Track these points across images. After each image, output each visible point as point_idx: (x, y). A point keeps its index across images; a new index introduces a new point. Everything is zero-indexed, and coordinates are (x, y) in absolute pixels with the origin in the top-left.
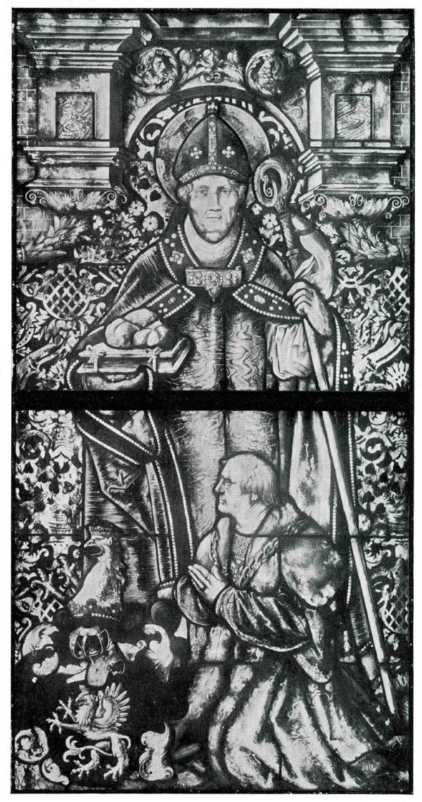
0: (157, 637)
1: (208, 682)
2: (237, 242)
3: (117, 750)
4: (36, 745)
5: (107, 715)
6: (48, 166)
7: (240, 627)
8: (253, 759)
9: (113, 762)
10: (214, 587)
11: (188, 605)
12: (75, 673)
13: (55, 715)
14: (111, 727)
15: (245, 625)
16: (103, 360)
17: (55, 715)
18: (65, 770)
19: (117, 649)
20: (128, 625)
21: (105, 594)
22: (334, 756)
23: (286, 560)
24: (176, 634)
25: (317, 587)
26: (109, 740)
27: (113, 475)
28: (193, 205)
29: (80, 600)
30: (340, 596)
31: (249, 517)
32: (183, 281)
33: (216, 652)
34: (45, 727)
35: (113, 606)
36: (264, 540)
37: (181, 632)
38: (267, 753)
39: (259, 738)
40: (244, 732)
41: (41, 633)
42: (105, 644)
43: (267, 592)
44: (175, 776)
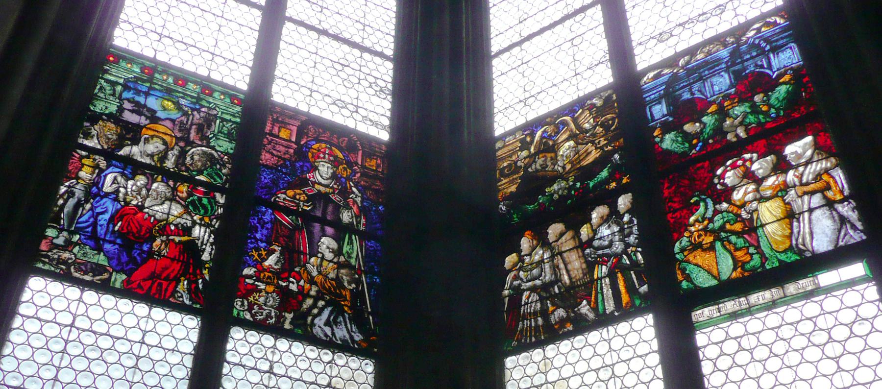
0: (293, 283)
1: (309, 302)
3: (273, 314)
4: (243, 305)
9: (272, 318)
10: (315, 273)
11: (305, 276)
12: (262, 286)
14: (272, 307)
15: (324, 288)
16: (284, 199)
18: (252, 316)
21: (276, 264)
22: (351, 337)
25: (350, 283)
29: (267, 263)
30: (357, 288)
31: (329, 256)
32: (313, 187)
33: (313, 293)
34: (248, 300)
37: (302, 283)
38: (328, 330)
39: (325, 325)
40: (320, 321)
43: (332, 279)
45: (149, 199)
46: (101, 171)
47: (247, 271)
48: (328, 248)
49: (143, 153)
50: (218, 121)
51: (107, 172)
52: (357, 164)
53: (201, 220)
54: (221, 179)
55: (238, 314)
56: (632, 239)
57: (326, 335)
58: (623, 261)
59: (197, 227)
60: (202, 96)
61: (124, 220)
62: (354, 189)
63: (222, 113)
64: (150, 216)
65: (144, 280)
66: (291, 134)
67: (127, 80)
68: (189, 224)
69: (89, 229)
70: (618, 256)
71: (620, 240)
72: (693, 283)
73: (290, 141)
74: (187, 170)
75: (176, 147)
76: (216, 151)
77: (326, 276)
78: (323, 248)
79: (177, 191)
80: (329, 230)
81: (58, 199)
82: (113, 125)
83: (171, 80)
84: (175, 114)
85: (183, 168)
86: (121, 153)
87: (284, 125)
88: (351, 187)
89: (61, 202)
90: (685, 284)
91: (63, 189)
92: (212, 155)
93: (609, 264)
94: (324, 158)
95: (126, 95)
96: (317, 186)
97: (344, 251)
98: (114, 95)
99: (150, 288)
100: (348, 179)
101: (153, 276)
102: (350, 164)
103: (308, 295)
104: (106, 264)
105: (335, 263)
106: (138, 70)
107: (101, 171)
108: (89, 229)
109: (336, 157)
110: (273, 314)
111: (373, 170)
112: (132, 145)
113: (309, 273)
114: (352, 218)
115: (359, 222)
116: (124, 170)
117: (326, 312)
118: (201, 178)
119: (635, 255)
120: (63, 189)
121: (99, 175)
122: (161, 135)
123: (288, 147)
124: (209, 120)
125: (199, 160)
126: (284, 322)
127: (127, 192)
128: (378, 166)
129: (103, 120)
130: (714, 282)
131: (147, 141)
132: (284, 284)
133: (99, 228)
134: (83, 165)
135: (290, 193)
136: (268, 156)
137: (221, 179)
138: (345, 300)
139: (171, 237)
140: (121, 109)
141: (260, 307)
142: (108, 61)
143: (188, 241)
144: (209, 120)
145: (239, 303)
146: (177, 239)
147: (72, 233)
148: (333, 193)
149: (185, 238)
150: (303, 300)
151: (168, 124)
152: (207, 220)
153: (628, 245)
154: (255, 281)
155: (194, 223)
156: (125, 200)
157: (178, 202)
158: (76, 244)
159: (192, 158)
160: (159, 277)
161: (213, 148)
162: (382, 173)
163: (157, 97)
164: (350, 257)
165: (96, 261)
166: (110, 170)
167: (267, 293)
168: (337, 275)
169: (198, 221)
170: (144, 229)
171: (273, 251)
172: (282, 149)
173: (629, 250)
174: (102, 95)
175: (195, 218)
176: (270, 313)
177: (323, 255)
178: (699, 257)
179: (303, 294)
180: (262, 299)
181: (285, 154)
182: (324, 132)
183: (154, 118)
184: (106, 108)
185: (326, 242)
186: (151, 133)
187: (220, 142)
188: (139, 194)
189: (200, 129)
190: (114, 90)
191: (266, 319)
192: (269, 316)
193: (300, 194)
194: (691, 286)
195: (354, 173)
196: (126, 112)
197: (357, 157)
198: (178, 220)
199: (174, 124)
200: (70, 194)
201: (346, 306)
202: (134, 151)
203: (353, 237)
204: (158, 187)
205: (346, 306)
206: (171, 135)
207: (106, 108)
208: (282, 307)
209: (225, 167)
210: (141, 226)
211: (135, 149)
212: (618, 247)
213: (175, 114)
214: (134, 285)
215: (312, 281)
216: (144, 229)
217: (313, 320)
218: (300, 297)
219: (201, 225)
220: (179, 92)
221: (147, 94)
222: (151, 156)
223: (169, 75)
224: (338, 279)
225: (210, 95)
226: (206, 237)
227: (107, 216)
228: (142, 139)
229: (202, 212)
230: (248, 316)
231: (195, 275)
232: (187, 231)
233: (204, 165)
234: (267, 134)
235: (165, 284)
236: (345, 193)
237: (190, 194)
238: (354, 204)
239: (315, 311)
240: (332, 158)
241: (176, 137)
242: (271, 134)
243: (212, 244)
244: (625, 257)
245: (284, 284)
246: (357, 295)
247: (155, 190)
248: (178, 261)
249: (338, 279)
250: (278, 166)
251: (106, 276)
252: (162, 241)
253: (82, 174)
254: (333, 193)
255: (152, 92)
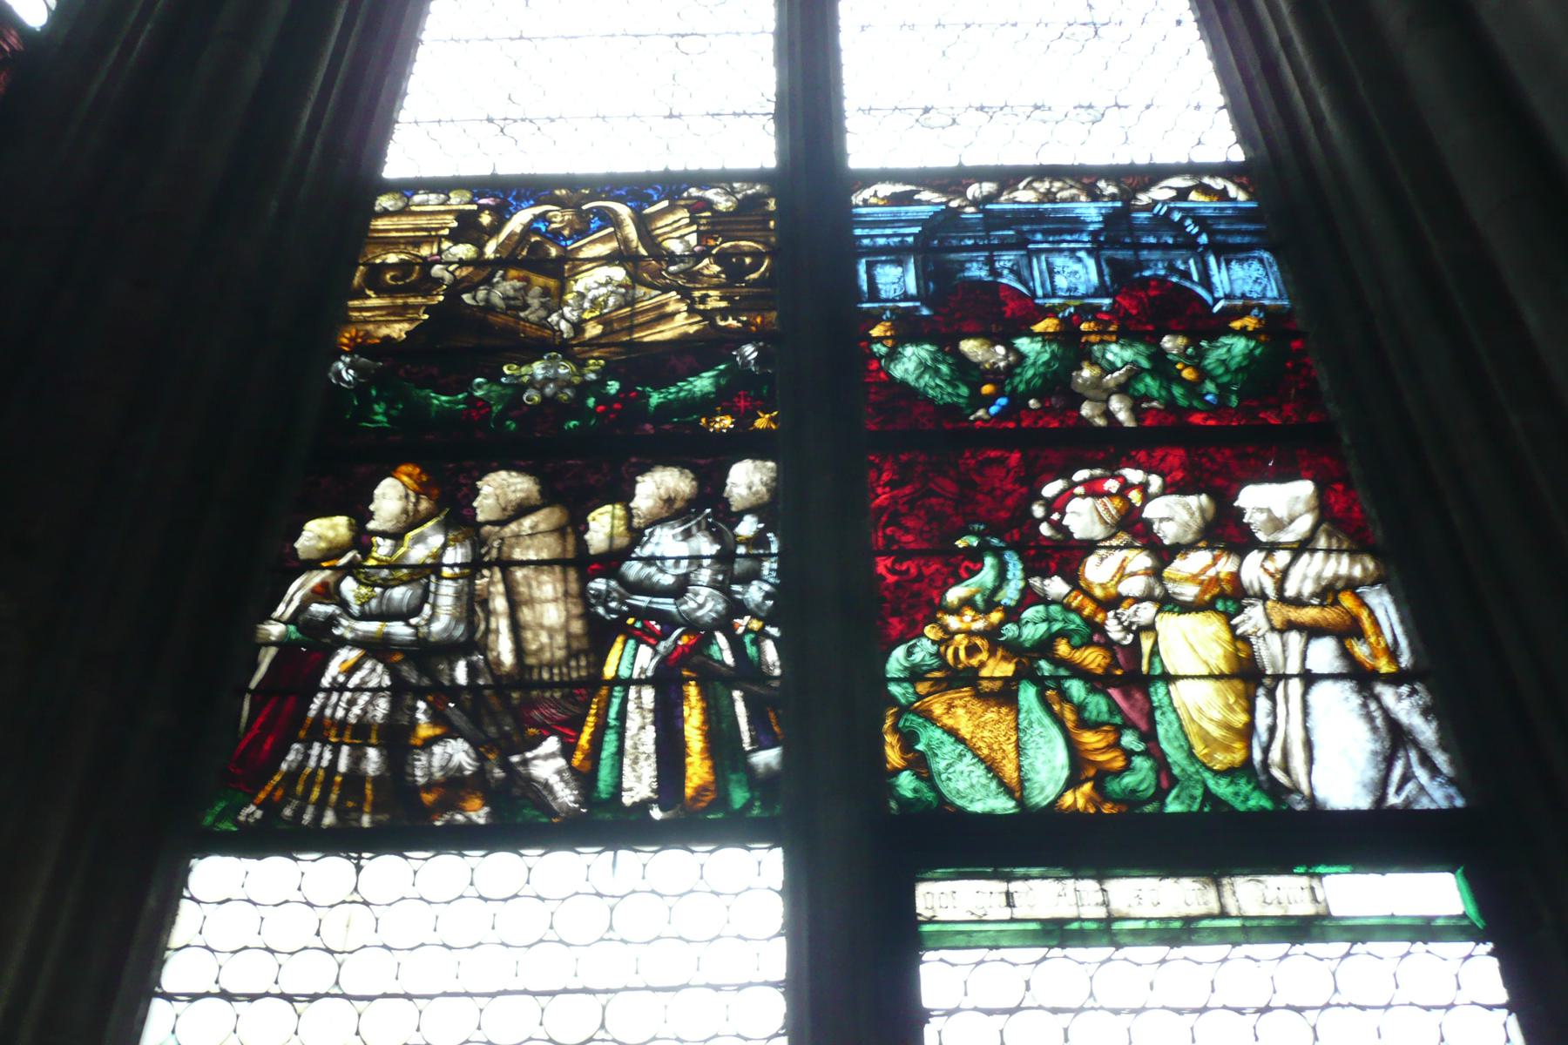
56: (755, 593)
58: (714, 650)
70: (702, 632)
71: (713, 584)
72: (934, 788)
90: (906, 783)
93: (663, 646)
119: (756, 642)
130: (1004, 805)
153: (737, 608)
173: (741, 623)
178: (962, 713)
194: (929, 796)
212: (704, 602)
244: (721, 638)
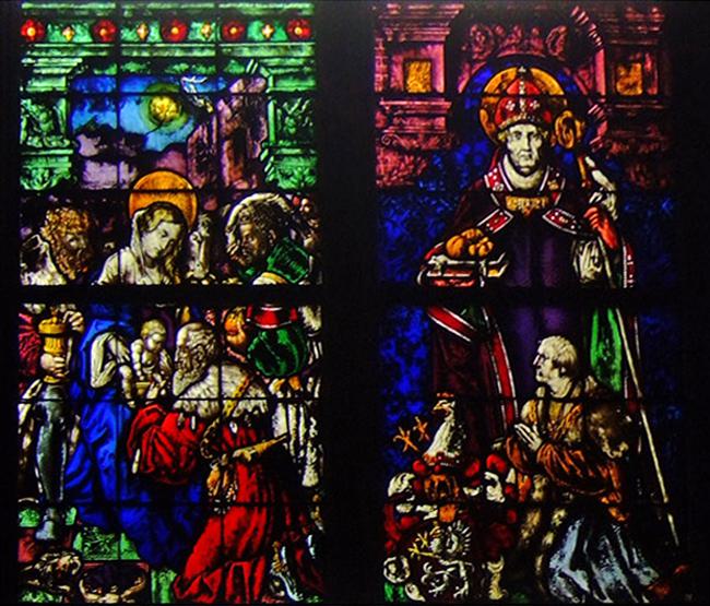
1: (534, 519)
2: (543, 176)
3: (463, 574)
5: (454, 547)
6: (398, 116)
7: (556, 476)
8: (570, 583)
11: (515, 457)
13: (415, 545)
14: (457, 556)
16: (445, 267)
17: (415, 545)
18: (423, 590)
19: (461, 492)
20: (470, 473)
21: (451, 448)
22: (633, 580)
23: (590, 420)
24: (508, 480)
25: (614, 447)
26: (457, 566)
27: (454, 352)
28: (510, 146)
29: (432, 452)
30: (633, 447)
31: (561, 386)
32: (503, 207)
35: (457, 458)
36: (572, 405)
37: (511, 477)
41: (402, 480)
42: (453, 487)
43: (575, 446)
44: (510, 596)
45: (177, 375)
46: (79, 337)
47: (396, 485)
48: (556, 364)
49: (145, 262)
50: (271, 107)
51: (88, 339)
52: (595, 96)
53: (284, 388)
54: (305, 265)
55: (396, 594)
57: (577, 590)
59: (280, 410)
60: (226, 47)
61: (144, 442)
62: (598, 175)
63: (276, 78)
64: (188, 415)
65: (209, 570)
66: (432, 73)
67: (72, 78)
68: (263, 405)
69: (89, 487)
73: (433, 94)
74: (236, 270)
75: (203, 218)
76: (282, 193)
77: (560, 443)
78: (546, 371)
79: (226, 333)
80: (552, 317)
81: (22, 436)
82: (72, 214)
83: (155, 35)
84: (182, 128)
85: (226, 269)
86: (104, 278)
87: (412, 50)
88: (589, 170)
89: (27, 441)
91: (24, 409)
92: (275, 206)
94: (517, 110)
95: (82, 119)
96: (512, 203)
97: (593, 359)
98: (55, 131)
99: (222, 587)
100: (583, 148)
101: (222, 557)
102: (577, 101)
103: (532, 505)
104: (135, 557)
105: (575, 401)
106: (85, 38)
107: (79, 337)
108: (89, 487)
109: (544, 97)
110: (463, 574)
111: (636, 98)
112: (117, 250)
113: (524, 447)
114: (601, 262)
115: (617, 269)
116: (116, 318)
117: (572, 537)
118: (267, 279)
120: (24, 409)
121: (75, 349)
122: (166, 198)
123: (431, 115)
124: (251, 112)
125: (253, 233)
126: (489, 583)
127: (134, 372)
128: (647, 79)
129: (53, 207)
131: (143, 226)
132: (475, 493)
133: (105, 478)
134: (44, 336)
135: (454, 244)
136: (391, 158)
137: (305, 265)
138: (610, 490)
139: (237, 453)
140: (78, 162)
141: (436, 566)
142: (28, 44)
143: (269, 449)
144: (251, 112)
145: (393, 568)
146: (248, 453)
147: (62, 509)
148: (550, 206)
149: (261, 447)
150: (522, 519)
151: (174, 160)
152: (295, 384)
154: (415, 504)
155: (273, 402)
156: (134, 391)
157: (233, 362)
158: (75, 529)
159: (238, 235)
160: (233, 556)
161: (273, 187)
162: (660, 97)
163: (139, 97)
164: (608, 373)
165: (114, 556)
166: (92, 331)
167: (443, 526)
168: (585, 432)
169: (280, 395)
170: (183, 450)
171: (442, 414)
172: (420, 124)
174: (35, 142)
175: (272, 388)
176: (457, 572)
177: (548, 389)
179: (517, 503)
180: (435, 543)
181: (427, 137)
182: (508, 32)
183: (145, 161)
184: (51, 172)
185: (551, 353)
186: (146, 201)
187: (289, 165)
188: (157, 369)
189: (241, 152)
190: (54, 117)
191: (450, 589)
192: (455, 580)
193: (476, 240)
195: (590, 131)
196: (91, 167)
197: (593, 77)
198: (242, 405)
199: (186, 157)
200: (37, 414)
201: (613, 504)
202: (123, 263)
203: (610, 316)
204: (187, 339)
205: (613, 504)
206: (185, 191)
207: (51, 172)
208: (477, 555)
209: (305, 228)
210: (177, 445)
211: (127, 257)
213: (182, 128)
214: (194, 588)
215: (531, 466)
216: (183, 450)
217: (546, 562)
218: (513, 515)
219: (286, 402)
220: (179, 60)
221: (118, 99)
222: (158, 262)
223: (148, 22)
224: (589, 442)
225: (243, 37)
226: (302, 430)
227: (111, 447)
228: (134, 225)
229: (283, 366)
230: (415, 595)
231: (296, 527)
232: (261, 425)
233: (264, 243)
234: (380, 94)
235: (246, 566)
236: (576, 195)
237: (251, 330)
238: (600, 222)
239: (549, 539)
240: (535, 105)
241: (195, 190)
242: (390, 93)
243: (315, 442)
245: (475, 493)
246: (635, 466)
247: (184, 348)
248: (261, 505)
249: (589, 442)
250: (416, 180)
251: (140, 583)
252: (222, 469)
253: (47, 361)
254: (550, 206)
255: (127, 89)
